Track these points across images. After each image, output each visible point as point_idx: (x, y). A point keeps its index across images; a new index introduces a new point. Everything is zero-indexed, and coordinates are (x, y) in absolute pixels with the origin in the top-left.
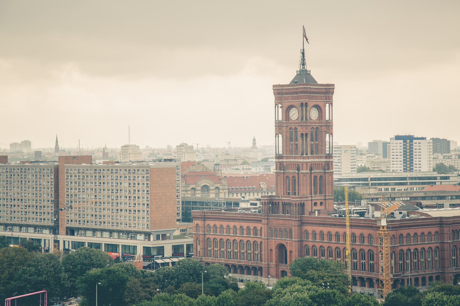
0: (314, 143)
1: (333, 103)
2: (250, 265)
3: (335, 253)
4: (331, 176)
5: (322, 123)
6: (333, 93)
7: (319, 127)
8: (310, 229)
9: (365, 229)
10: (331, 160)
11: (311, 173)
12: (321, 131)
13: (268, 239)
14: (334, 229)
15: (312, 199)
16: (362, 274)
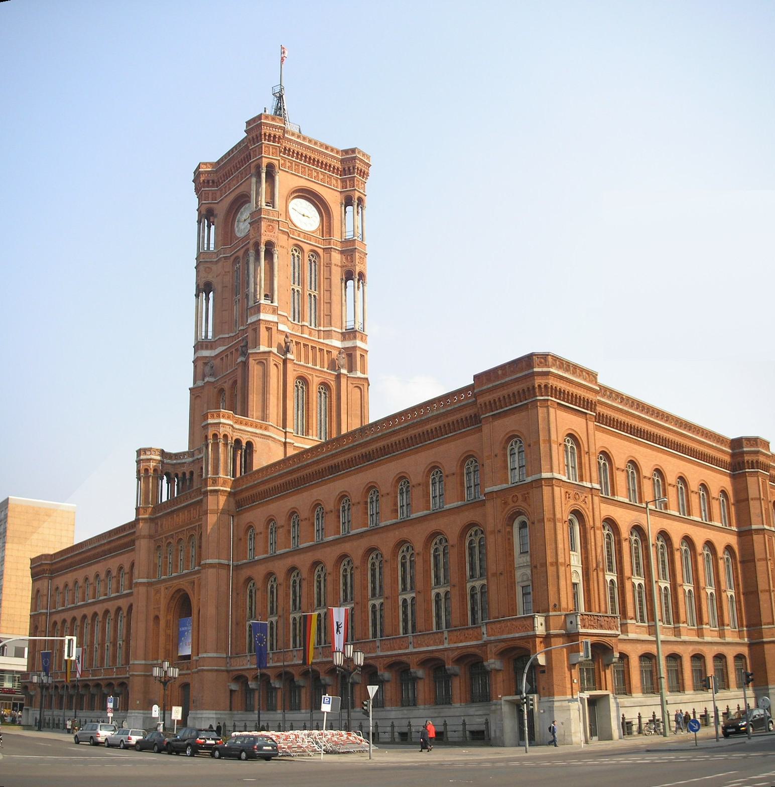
0: (303, 289)
1: (367, 201)
2: (114, 679)
3: (336, 582)
4: (358, 390)
5: (330, 244)
6: (364, 174)
7: (320, 251)
8: (257, 516)
9: (447, 441)
10: (359, 343)
11: (285, 362)
12: (329, 265)
13: (149, 584)
14: (331, 485)
15: (288, 440)
16: (435, 644)
